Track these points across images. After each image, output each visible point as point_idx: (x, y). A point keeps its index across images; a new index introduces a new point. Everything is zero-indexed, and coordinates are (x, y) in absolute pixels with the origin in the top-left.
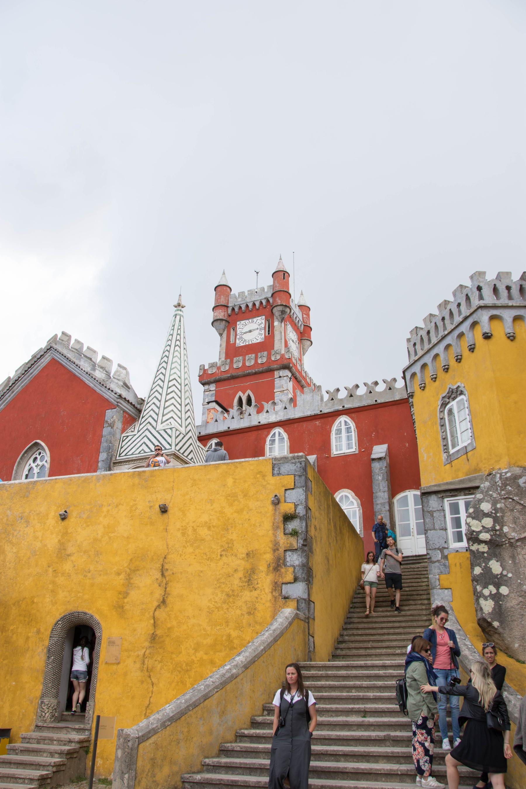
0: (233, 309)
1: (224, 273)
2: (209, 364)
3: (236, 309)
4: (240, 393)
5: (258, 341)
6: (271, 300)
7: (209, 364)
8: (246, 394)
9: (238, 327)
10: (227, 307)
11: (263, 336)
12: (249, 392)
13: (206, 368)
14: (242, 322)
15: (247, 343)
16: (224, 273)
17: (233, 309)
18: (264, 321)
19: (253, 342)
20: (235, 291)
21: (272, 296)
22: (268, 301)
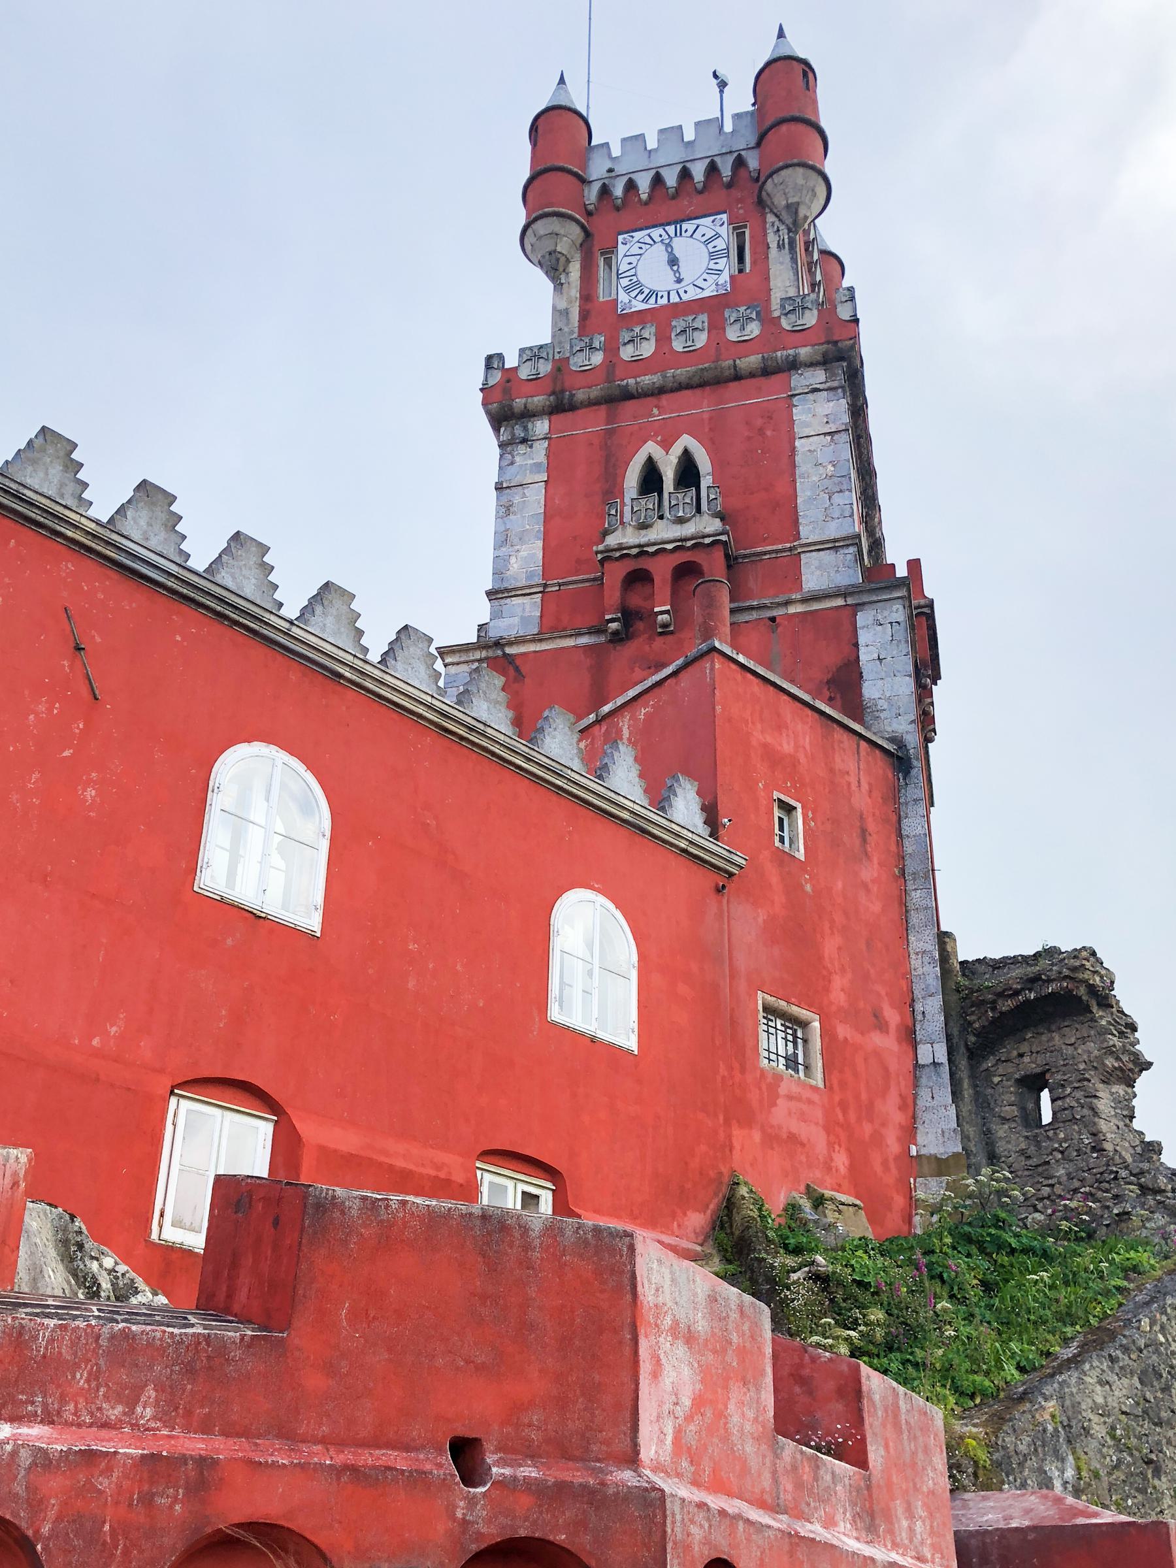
0: (605, 191)
1: (562, 81)
2: (522, 351)
3: (618, 191)
4: (651, 448)
5: (706, 294)
6: (753, 162)
7: (522, 351)
8: (677, 450)
9: (622, 250)
10: (583, 181)
11: (725, 277)
12: (687, 441)
13: (511, 362)
14: (638, 235)
15: (664, 301)
16: (562, 81)
17: (605, 191)
18: (723, 231)
19: (685, 297)
20: (608, 130)
21: (759, 144)
22: (740, 162)
